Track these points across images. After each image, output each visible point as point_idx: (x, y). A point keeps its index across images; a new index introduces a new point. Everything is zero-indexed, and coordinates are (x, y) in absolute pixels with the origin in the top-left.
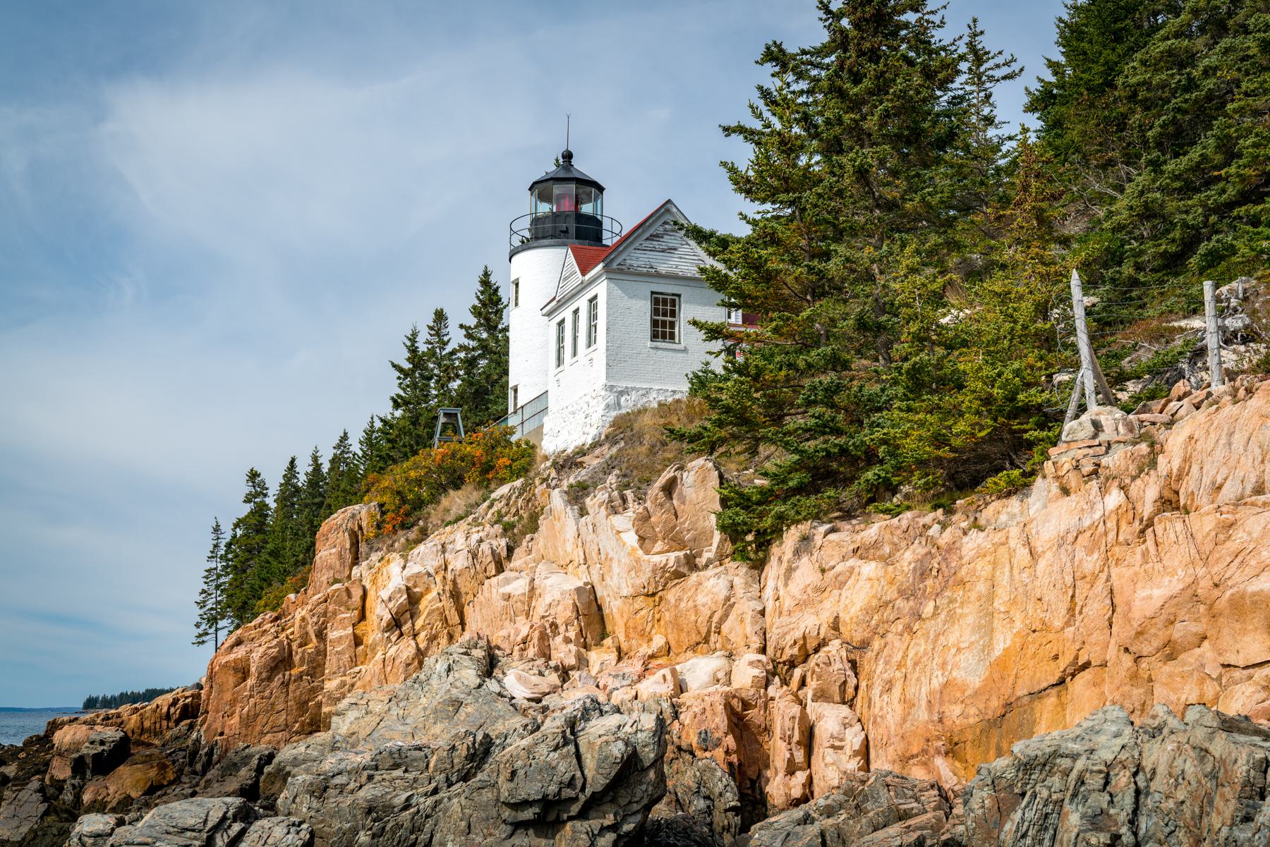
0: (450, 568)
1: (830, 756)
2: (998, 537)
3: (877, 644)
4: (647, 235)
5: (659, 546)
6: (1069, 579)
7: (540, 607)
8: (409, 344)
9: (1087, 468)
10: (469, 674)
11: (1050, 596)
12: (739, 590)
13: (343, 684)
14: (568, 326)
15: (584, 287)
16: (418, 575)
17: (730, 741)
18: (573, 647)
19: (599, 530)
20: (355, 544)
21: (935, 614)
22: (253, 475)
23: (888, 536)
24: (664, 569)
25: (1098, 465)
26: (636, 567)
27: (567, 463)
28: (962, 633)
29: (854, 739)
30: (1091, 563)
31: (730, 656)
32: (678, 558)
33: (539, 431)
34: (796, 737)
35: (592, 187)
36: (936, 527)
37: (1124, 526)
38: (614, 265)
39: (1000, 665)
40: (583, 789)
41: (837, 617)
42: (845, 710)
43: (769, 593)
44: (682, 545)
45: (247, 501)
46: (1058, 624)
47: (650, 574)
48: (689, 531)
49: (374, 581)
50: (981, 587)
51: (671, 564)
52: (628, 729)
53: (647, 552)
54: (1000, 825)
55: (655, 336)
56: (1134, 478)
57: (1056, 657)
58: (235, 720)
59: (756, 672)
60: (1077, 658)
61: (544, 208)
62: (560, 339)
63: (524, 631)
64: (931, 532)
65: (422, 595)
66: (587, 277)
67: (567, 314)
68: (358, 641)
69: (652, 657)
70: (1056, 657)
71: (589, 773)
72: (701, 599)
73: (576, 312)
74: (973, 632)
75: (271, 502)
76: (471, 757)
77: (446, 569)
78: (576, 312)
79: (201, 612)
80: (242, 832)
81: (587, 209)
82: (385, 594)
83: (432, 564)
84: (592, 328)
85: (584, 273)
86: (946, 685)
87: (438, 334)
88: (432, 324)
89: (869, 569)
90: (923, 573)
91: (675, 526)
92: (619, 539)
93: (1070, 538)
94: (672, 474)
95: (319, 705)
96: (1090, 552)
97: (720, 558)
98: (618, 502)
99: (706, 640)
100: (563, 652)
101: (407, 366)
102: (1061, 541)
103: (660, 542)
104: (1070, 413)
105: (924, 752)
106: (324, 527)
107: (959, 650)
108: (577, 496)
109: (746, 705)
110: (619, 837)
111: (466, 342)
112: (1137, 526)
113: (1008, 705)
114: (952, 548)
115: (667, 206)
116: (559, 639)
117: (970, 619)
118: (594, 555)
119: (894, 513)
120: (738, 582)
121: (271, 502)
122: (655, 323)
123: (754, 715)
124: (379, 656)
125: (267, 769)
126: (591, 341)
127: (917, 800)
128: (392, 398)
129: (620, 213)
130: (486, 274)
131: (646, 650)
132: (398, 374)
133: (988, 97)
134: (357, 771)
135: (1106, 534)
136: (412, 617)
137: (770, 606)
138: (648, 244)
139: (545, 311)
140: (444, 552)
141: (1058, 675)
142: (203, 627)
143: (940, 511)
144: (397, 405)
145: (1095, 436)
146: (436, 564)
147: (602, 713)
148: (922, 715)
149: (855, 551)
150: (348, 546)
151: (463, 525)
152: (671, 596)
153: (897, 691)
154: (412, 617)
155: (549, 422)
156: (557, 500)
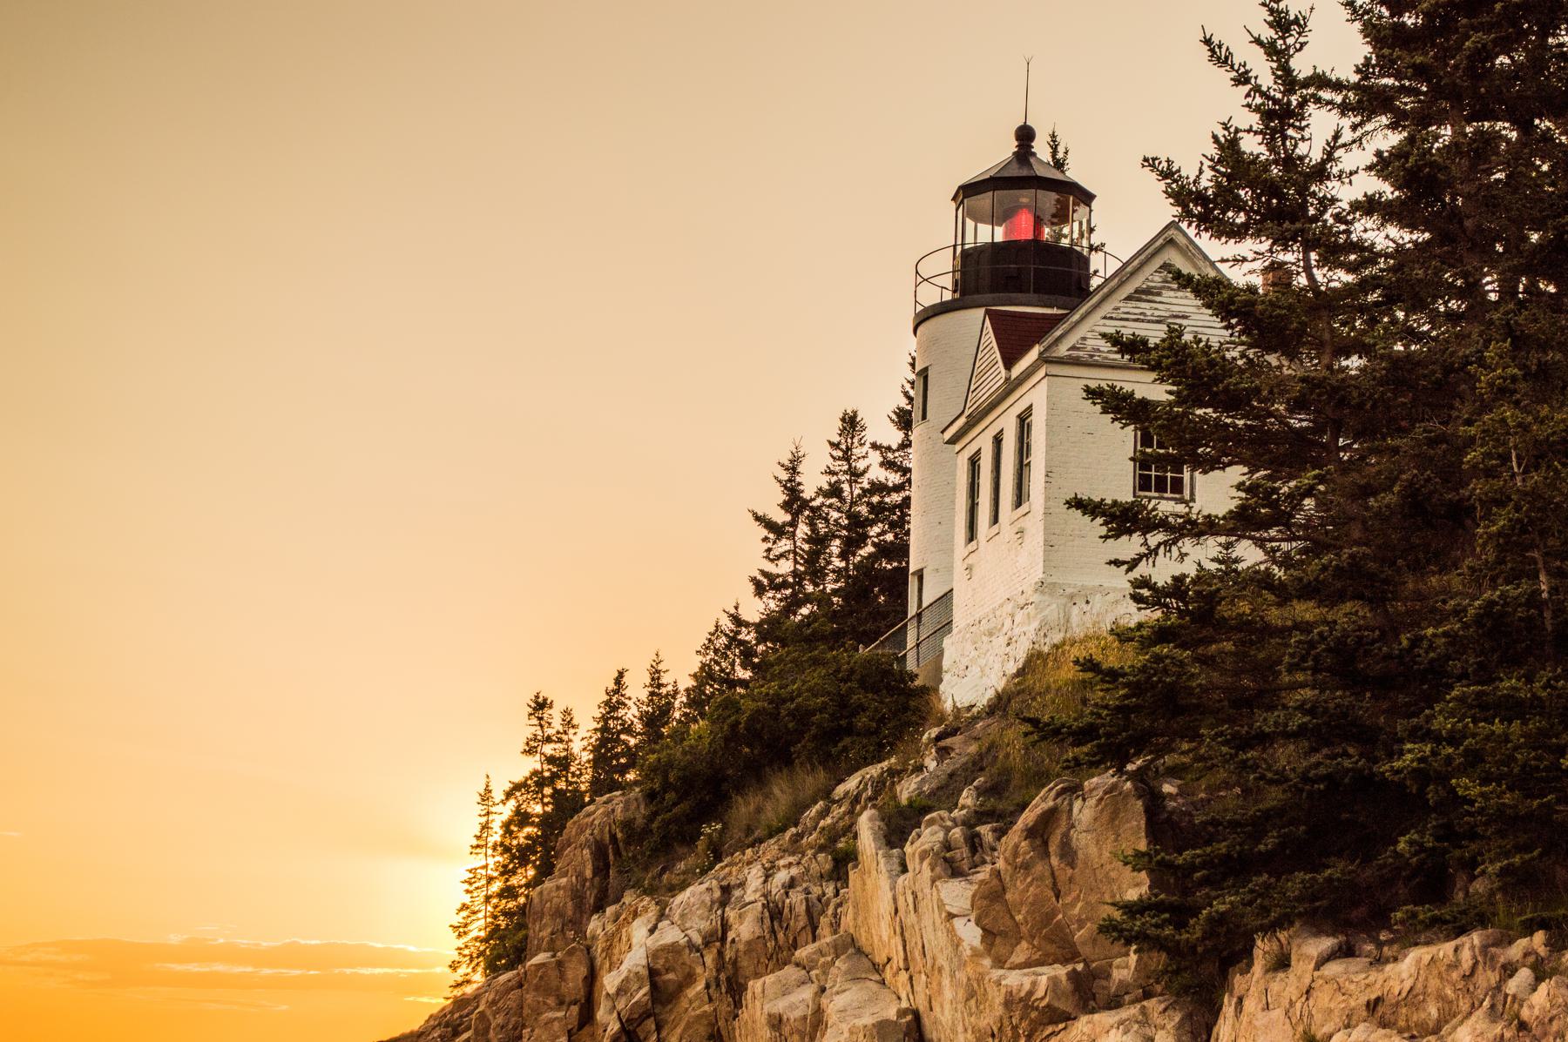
0: (731, 935)
4: (1129, 289)
5: (1020, 955)
8: (784, 476)
15: (1011, 387)
16: (673, 949)
19: (922, 906)
20: (601, 869)
22: (540, 705)
23: (1434, 983)
26: (973, 993)
32: (1054, 981)
38: (1062, 350)
44: (1069, 954)
45: (530, 751)
47: (999, 1010)
48: (1081, 923)
49: (608, 949)
51: (1040, 993)
53: (1000, 963)
61: (987, 234)
64: (1512, 986)
66: (1017, 370)
67: (982, 441)
73: (998, 440)
75: (577, 746)
77: (723, 939)
78: (998, 440)
79: (460, 943)
83: (698, 926)
85: (1009, 363)
87: (847, 456)
88: (836, 439)
91: (1054, 913)
92: (951, 932)
94: (1051, 804)
98: (963, 852)
101: (782, 517)
103: (1024, 944)
118: (917, 954)
126: (1019, 500)
128: (754, 580)
132: (765, 532)
136: (659, 1029)
138: (1130, 307)
139: (948, 435)
140: (723, 903)
142: (463, 970)
143: (1539, 937)
144: (760, 590)
146: (705, 925)
149: (1373, 1006)
150: (588, 873)
151: (771, 848)
154: (659, 1029)
155: (952, 647)
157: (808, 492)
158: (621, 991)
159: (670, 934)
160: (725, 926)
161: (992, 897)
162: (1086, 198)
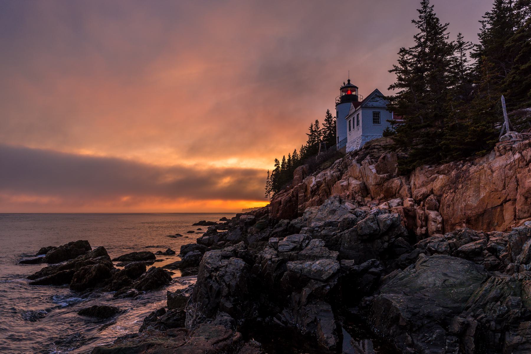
1: (433, 223)
2: (480, 167)
3: (445, 195)
5: (381, 173)
6: (503, 178)
7: (351, 188)
9: (508, 148)
10: (337, 203)
11: (498, 182)
12: (404, 183)
13: (302, 206)
14: (352, 122)
15: (356, 111)
16: (319, 181)
17: (405, 219)
18: (360, 197)
20: (303, 175)
21: (462, 188)
24: (383, 178)
25: (512, 147)
26: (376, 178)
27: (355, 153)
28: (470, 192)
29: (439, 219)
30: (511, 173)
31: (402, 199)
33: (345, 147)
34: (423, 218)
35: (355, 88)
36: (461, 165)
37: (521, 163)
39: (483, 200)
40: (380, 232)
41: (432, 189)
42: (436, 212)
43: (412, 183)
45: (275, 166)
46: (500, 189)
50: (476, 180)
52: (391, 217)
54: (522, 245)
55: (374, 122)
56: (523, 150)
57: (500, 198)
58: (279, 214)
59: (411, 203)
60: (506, 198)
62: (350, 125)
63: (348, 193)
64: (460, 167)
65: (320, 186)
67: (352, 119)
68: (305, 196)
69: (381, 199)
70: (500, 198)
71: (381, 228)
72: (393, 185)
73: (354, 118)
74: (474, 192)
75: (280, 166)
76: (349, 224)
80: (308, 243)
81: (354, 93)
82: (312, 185)
83: (322, 179)
84: (358, 121)
85: (356, 108)
86: (466, 206)
89: (441, 177)
90: (458, 177)
93: (503, 167)
95: (297, 211)
96: (510, 170)
97: (398, 175)
99: (395, 195)
100: (359, 198)
101: (310, 134)
102: (501, 167)
104: (501, 133)
105: (460, 222)
106: (295, 171)
107: (470, 197)
108: (359, 161)
109: (409, 211)
110: (389, 244)
111: (324, 127)
112: (525, 163)
113: (485, 211)
114: (467, 170)
115: (377, 91)
116: (357, 195)
117: (473, 189)
119: (447, 162)
120: (403, 181)
121: (280, 166)
122: (374, 119)
123: (410, 213)
124: (311, 200)
125: (289, 225)
127: (477, 236)
129: (362, 94)
130: (328, 111)
131: (378, 197)
133: (464, 54)
134: (319, 227)
135: (515, 165)
137: (412, 186)
141: (500, 203)
143: (462, 161)
145: (510, 140)
147: (382, 213)
148: (460, 213)
151: (329, 169)
152: (386, 184)
153: (451, 208)
156: (354, 162)
157: (314, 129)
158: (313, 186)
159: (319, 180)
160: (325, 178)
161: (377, 167)
162: (357, 88)
